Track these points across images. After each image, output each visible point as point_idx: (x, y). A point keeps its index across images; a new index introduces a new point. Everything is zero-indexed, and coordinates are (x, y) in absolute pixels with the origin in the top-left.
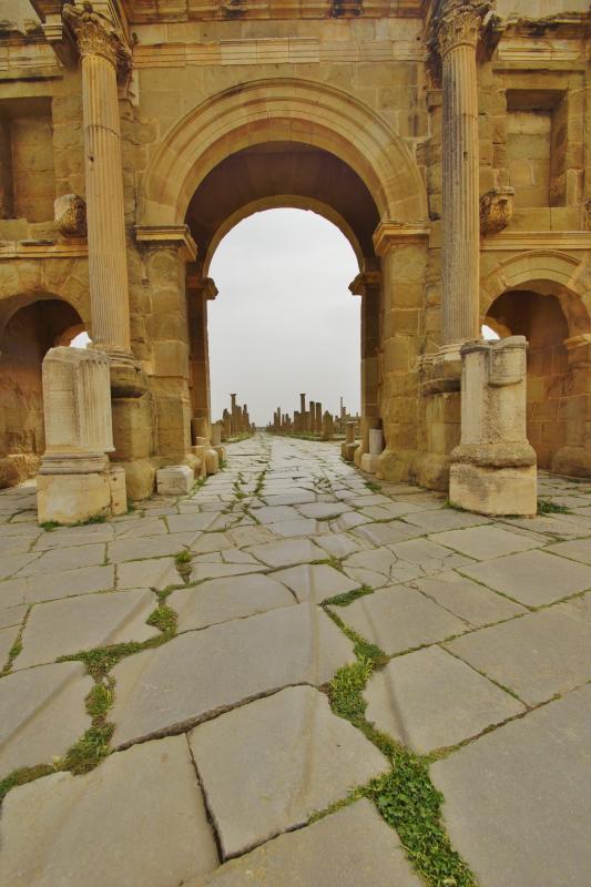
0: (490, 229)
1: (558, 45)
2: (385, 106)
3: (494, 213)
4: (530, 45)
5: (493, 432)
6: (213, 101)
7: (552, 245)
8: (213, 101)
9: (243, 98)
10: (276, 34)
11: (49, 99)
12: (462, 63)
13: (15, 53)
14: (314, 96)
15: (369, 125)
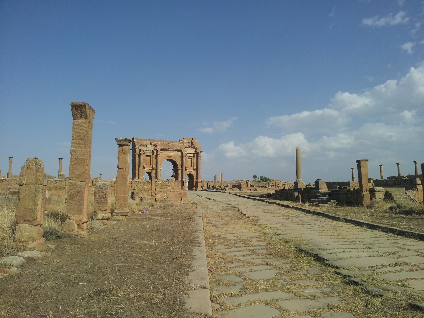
0: (186, 170)
1: (192, 154)
2: (178, 159)
3: (186, 169)
4: (189, 154)
5: (186, 185)
6: (165, 157)
7: (191, 171)
8: (165, 157)
9: (167, 157)
10: (170, 152)
11: (151, 156)
12: (184, 159)
13: (149, 152)
14: (173, 157)
15: (177, 160)
